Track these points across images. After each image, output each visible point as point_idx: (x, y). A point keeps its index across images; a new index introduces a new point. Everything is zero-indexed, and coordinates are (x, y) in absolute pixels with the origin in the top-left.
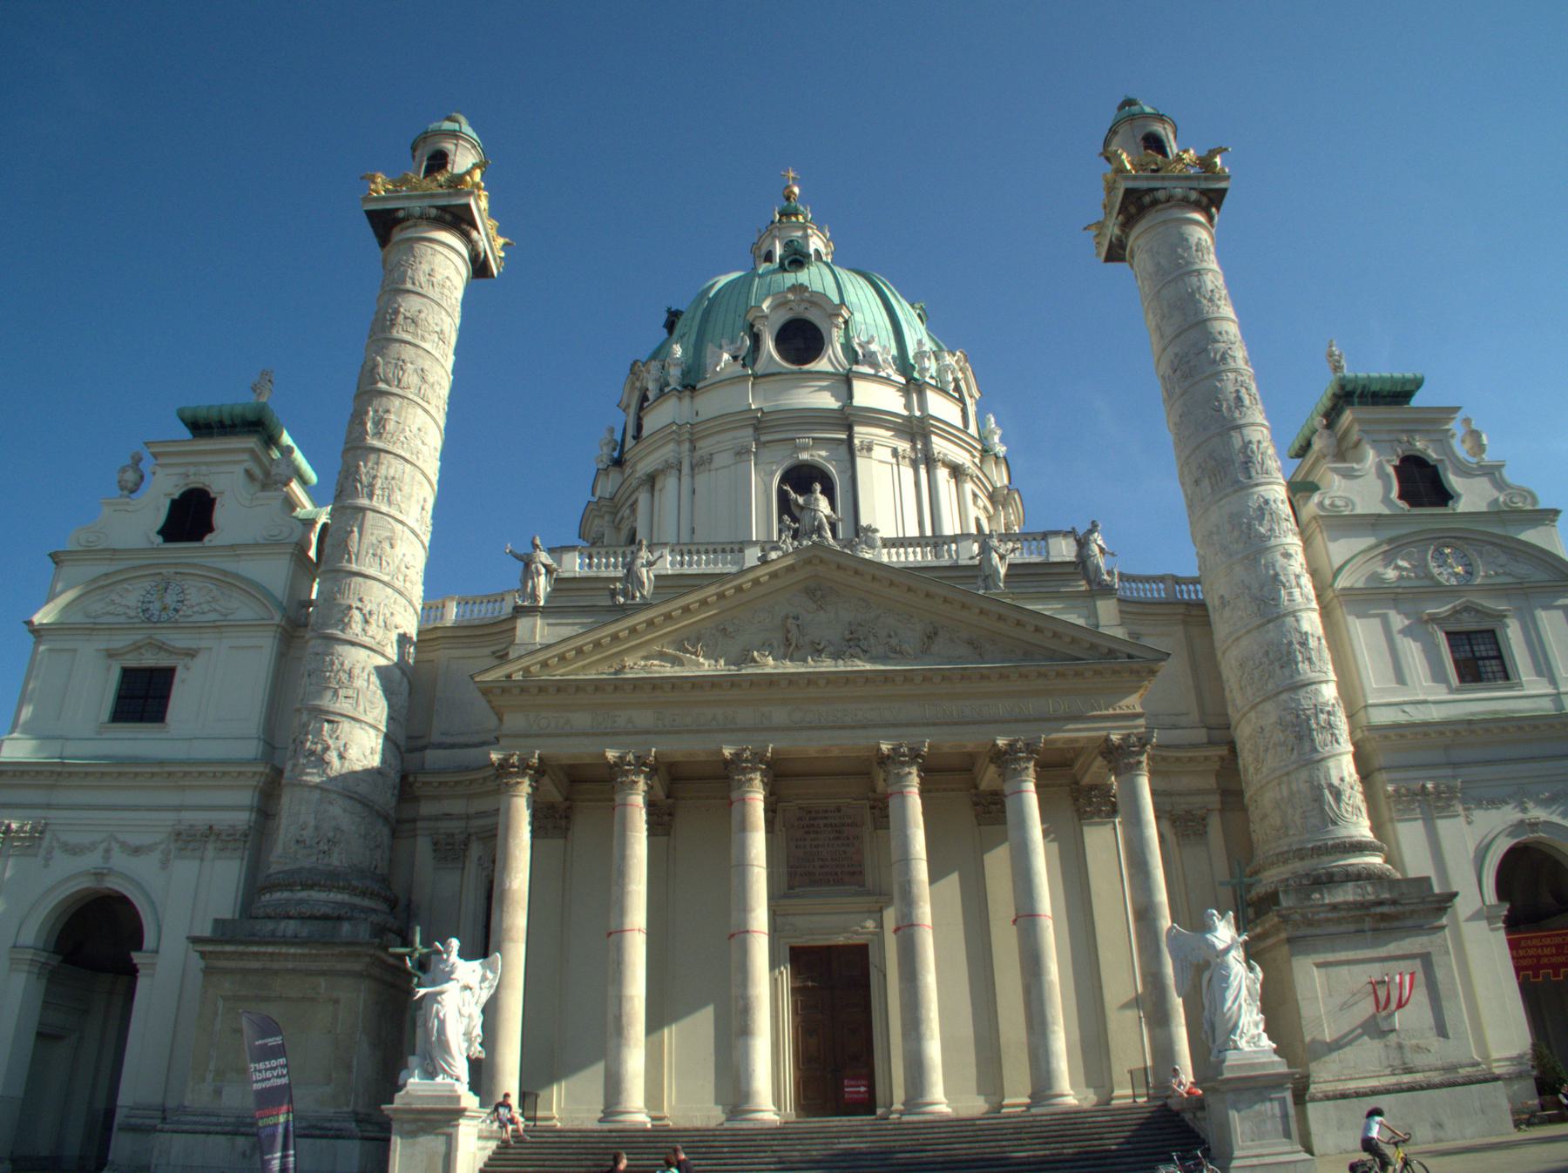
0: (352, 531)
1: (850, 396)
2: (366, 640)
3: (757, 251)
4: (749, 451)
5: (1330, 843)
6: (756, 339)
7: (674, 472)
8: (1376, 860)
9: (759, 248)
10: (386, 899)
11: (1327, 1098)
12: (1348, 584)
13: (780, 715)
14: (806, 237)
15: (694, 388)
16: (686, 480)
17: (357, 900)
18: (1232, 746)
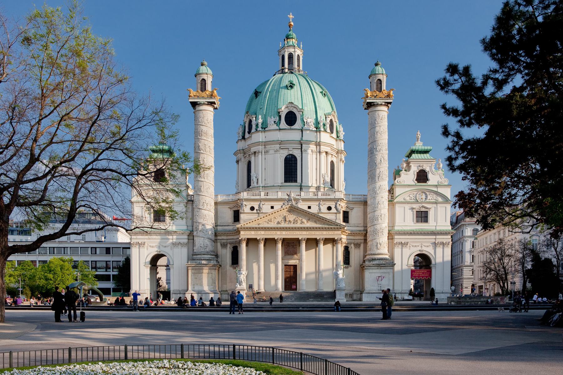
0: (201, 186)
1: (302, 136)
2: (208, 209)
3: (280, 52)
4: (278, 151)
5: (377, 253)
6: (280, 117)
7: (261, 153)
8: (387, 257)
9: (281, 51)
10: (215, 256)
11: (366, 293)
12: (398, 200)
13: (284, 233)
14: (295, 51)
15: (265, 128)
16: (264, 156)
17: (212, 256)
18: (367, 232)
